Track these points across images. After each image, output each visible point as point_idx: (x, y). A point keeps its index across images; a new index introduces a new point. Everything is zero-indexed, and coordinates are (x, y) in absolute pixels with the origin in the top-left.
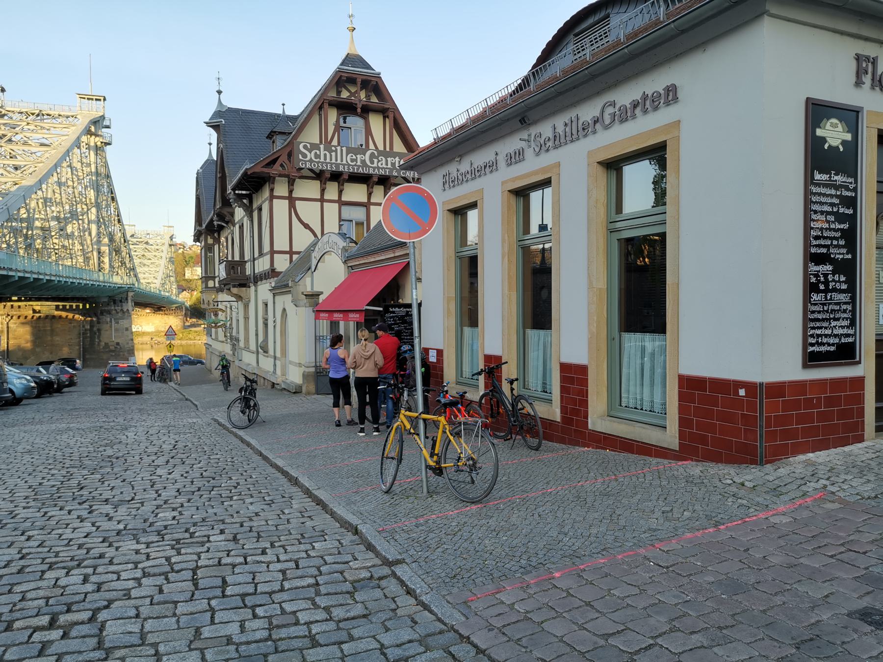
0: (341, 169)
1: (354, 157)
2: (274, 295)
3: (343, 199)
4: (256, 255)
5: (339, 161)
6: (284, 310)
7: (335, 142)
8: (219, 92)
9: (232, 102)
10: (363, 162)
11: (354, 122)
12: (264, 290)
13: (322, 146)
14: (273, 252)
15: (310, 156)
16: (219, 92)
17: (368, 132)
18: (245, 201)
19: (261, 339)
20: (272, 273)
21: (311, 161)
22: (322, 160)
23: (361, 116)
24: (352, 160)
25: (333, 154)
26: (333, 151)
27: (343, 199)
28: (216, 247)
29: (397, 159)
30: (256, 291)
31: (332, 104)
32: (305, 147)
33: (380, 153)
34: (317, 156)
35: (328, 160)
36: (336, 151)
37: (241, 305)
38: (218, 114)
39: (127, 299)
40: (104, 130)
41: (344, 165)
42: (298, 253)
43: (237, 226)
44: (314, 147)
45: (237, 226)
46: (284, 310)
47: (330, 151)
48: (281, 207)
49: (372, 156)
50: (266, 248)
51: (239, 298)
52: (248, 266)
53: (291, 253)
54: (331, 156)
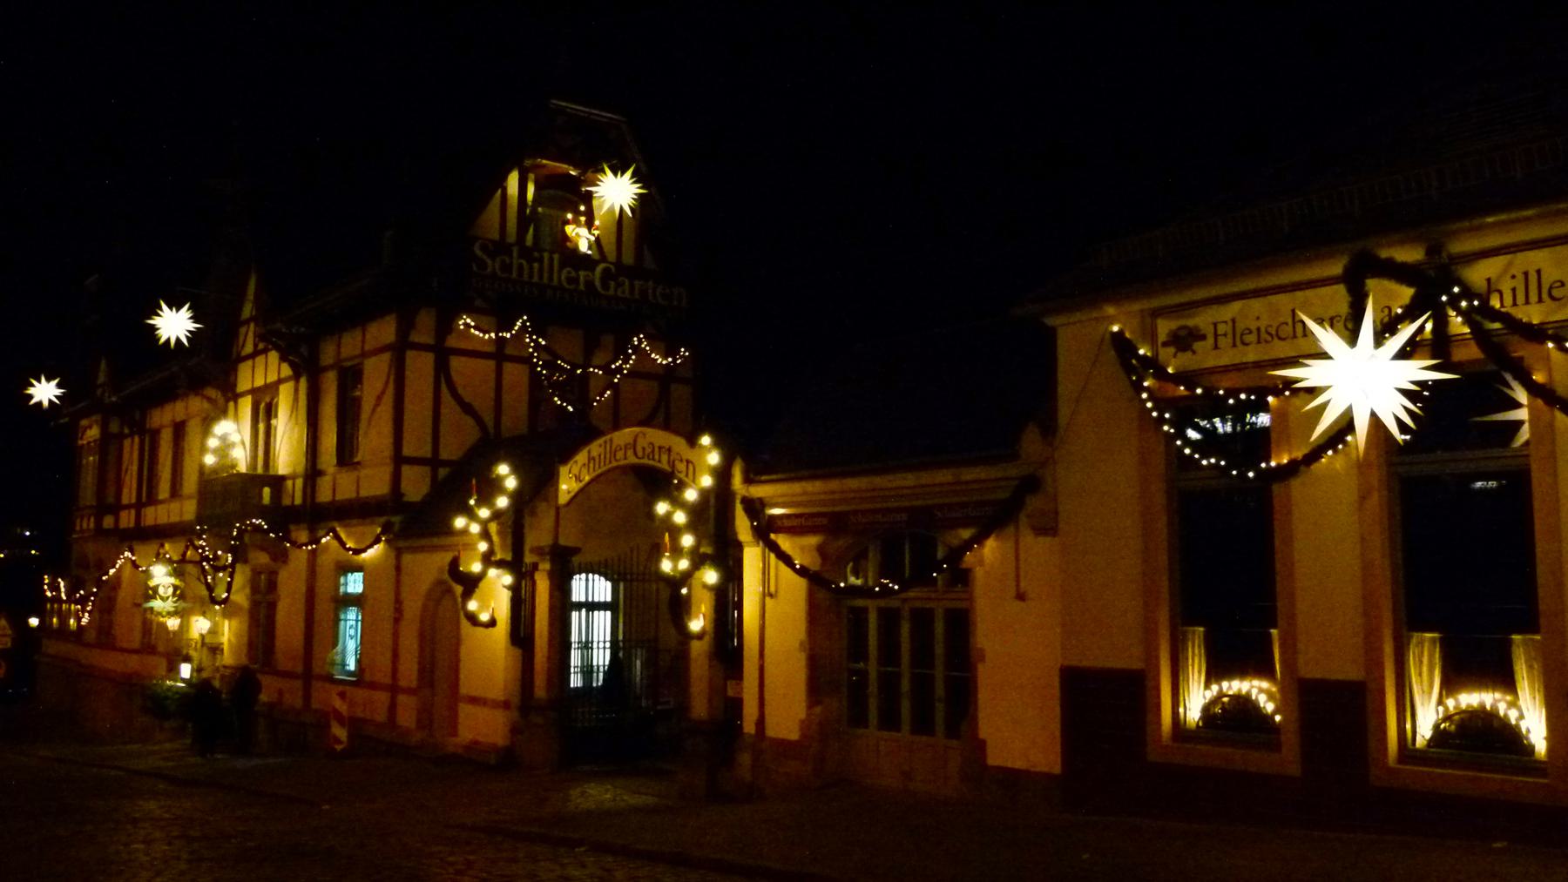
1: (573, 274)
10: (590, 284)
15: (493, 265)
22: (514, 275)
25: (536, 265)
26: (536, 260)
32: (484, 248)
34: (507, 268)
35: (526, 277)
36: (541, 260)
47: (531, 261)
54: (531, 268)
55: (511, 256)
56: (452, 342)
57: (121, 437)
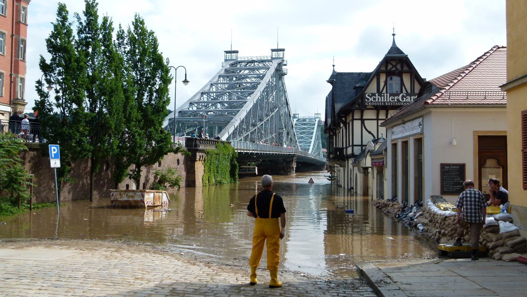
0: (386, 104)
2: (353, 167)
5: (385, 101)
7: (384, 91)
8: (334, 66)
9: (338, 70)
10: (398, 100)
11: (396, 80)
13: (377, 94)
14: (353, 146)
15: (371, 99)
16: (334, 66)
17: (402, 84)
21: (371, 102)
22: (377, 101)
24: (392, 100)
25: (383, 97)
31: (383, 72)
32: (369, 95)
34: (374, 99)
36: (384, 96)
37: (342, 169)
38: (332, 77)
39: (292, 161)
40: (283, 67)
41: (388, 102)
44: (373, 95)
47: (381, 96)
48: (357, 124)
49: (403, 97)
50: (351, 144)
51: (341, 166)
55: (375, 96)
56: (364, 118)
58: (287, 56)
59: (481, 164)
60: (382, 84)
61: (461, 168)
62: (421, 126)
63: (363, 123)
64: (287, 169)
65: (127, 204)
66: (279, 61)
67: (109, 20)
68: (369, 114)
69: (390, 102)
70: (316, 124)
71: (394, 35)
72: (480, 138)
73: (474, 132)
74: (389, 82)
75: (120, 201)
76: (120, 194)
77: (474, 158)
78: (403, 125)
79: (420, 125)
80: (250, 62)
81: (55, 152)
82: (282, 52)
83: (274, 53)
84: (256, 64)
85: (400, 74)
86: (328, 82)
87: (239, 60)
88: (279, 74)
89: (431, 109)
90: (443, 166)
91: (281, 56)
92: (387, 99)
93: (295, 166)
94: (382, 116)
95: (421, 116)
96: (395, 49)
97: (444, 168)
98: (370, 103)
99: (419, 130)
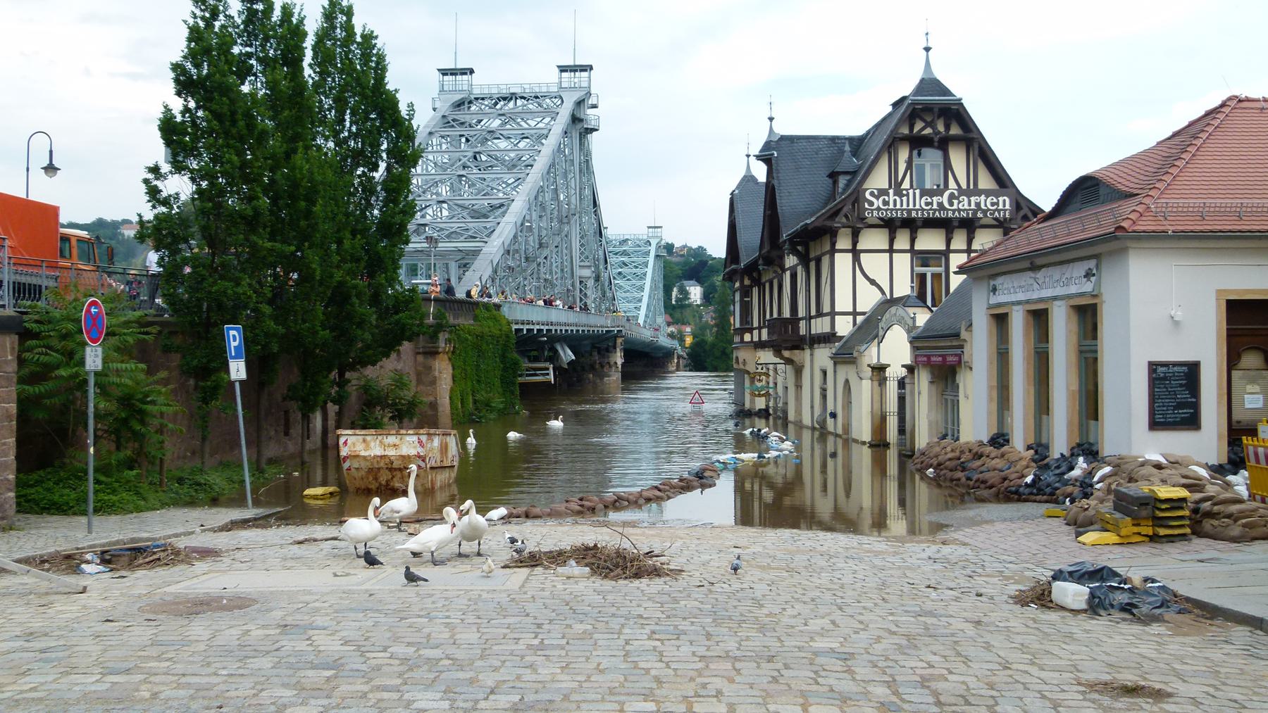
0: (914, 214)
2: (835, 364)
3: (917, 247)
4: (813, 313)
5: (911, 206)
6: (847, 381)
7: (906, 185)
8: (771, 119)
9: (783, 129)
11: (931, 156)
12: (823, 356)
13: (891, 192)
14: (833, 314)
15: (878, 203)
16: (771, 119)
17: (948, 166)
18: (799, 248)
19: (817, 411)
20: (830, 338)
21: (879, 209)
22: (891, 206)
23: (939, 148)
24: (927, 204)
25: (905, 199)
27: (917, 247)
28: (755, 291)
29: (983, 197)
30: (812, 355)
32: (872, 194)
33: (961, 192)
34: (886, 203)
35: (898, 206)
36: (908, 195)
38: (768, 146)
40: (590, 111)
42: (863, 314)
43: (788, 273)
44: (883, 192)
45: (788, 273)
46: (847, 381)
47: (901, 195)
49: (952, 197)
51: (789, 361)
52: (802, 324)
53: (855, 313)
55: (888, 195)
57: (751, 287)
58: (599, 83)
59: (1232, 360)
60: (902, 167)
61: (1192, 371)
62: (1093, 279)
63: (856, 259)
64: (602, 367)
65: (382, 465)
66: (576, 96)
67: (296, 11)
68: (873, 239)
69: (923, 210)
70: (652, 254)
71: (927, 49)
72: (1229, 302)
73: (1219, 292)
74: (916, 161)
75: (364, 457)
76: (364, 441)
77: (1219, 349)
78: (1031, 274)
79: (1088, 275)
80: (504, 99)
81: (236, 344)
82: (585, 74)
83: (564, 74)
84: (519, 102)
85: (943, 144)
86: (758, 157)
87: (477, 92)
88: (580, 127)
89: (1129, 244)
90: (1153, 367)
91: (585, 84)
92: (916, 204)
93: (620, 361)
94: (902, 242)
95: (1096, 257)
96: (929, 84)
97: (1155, 371)
98: (875, 213)
99: (1088, 287)
